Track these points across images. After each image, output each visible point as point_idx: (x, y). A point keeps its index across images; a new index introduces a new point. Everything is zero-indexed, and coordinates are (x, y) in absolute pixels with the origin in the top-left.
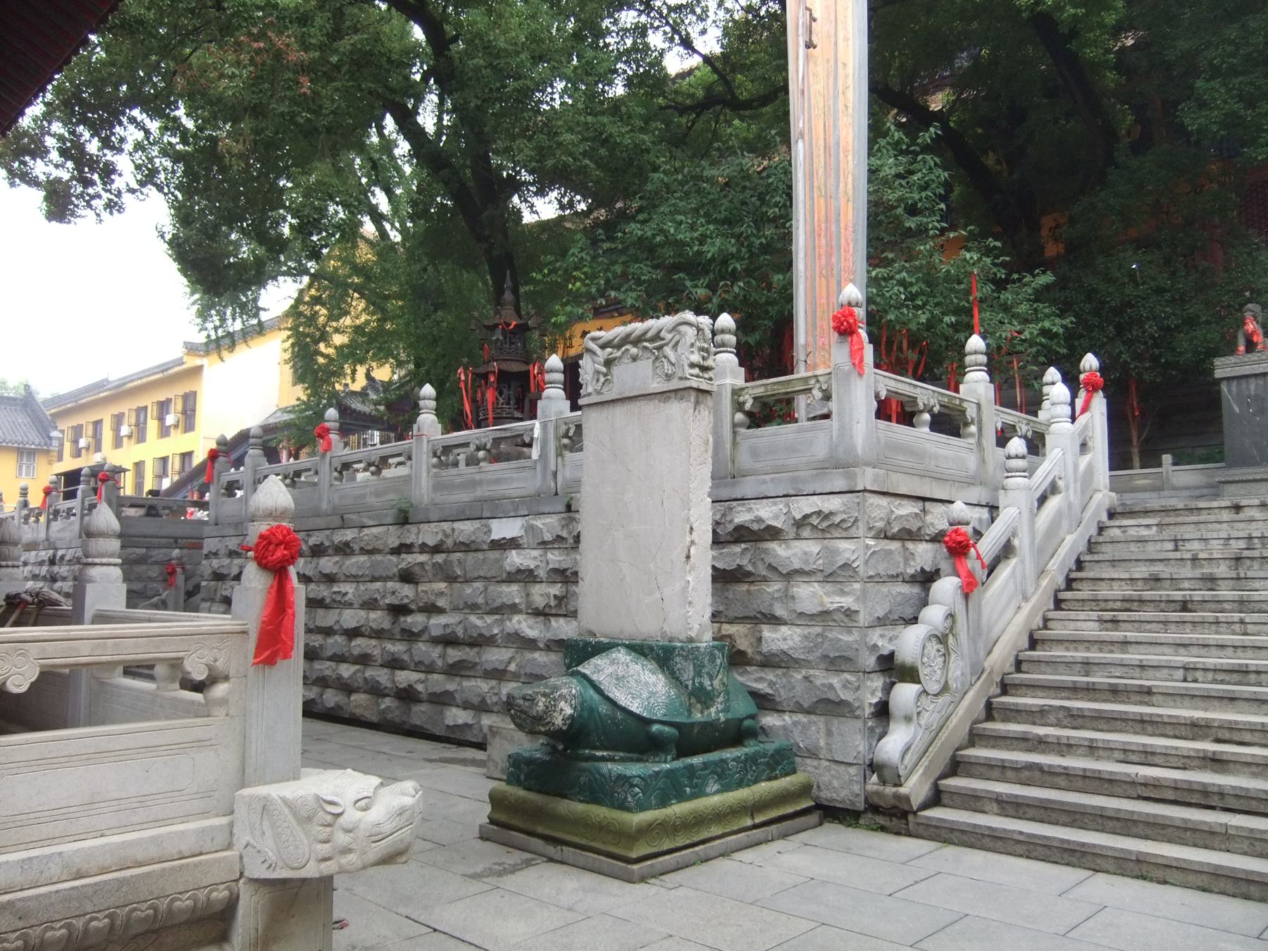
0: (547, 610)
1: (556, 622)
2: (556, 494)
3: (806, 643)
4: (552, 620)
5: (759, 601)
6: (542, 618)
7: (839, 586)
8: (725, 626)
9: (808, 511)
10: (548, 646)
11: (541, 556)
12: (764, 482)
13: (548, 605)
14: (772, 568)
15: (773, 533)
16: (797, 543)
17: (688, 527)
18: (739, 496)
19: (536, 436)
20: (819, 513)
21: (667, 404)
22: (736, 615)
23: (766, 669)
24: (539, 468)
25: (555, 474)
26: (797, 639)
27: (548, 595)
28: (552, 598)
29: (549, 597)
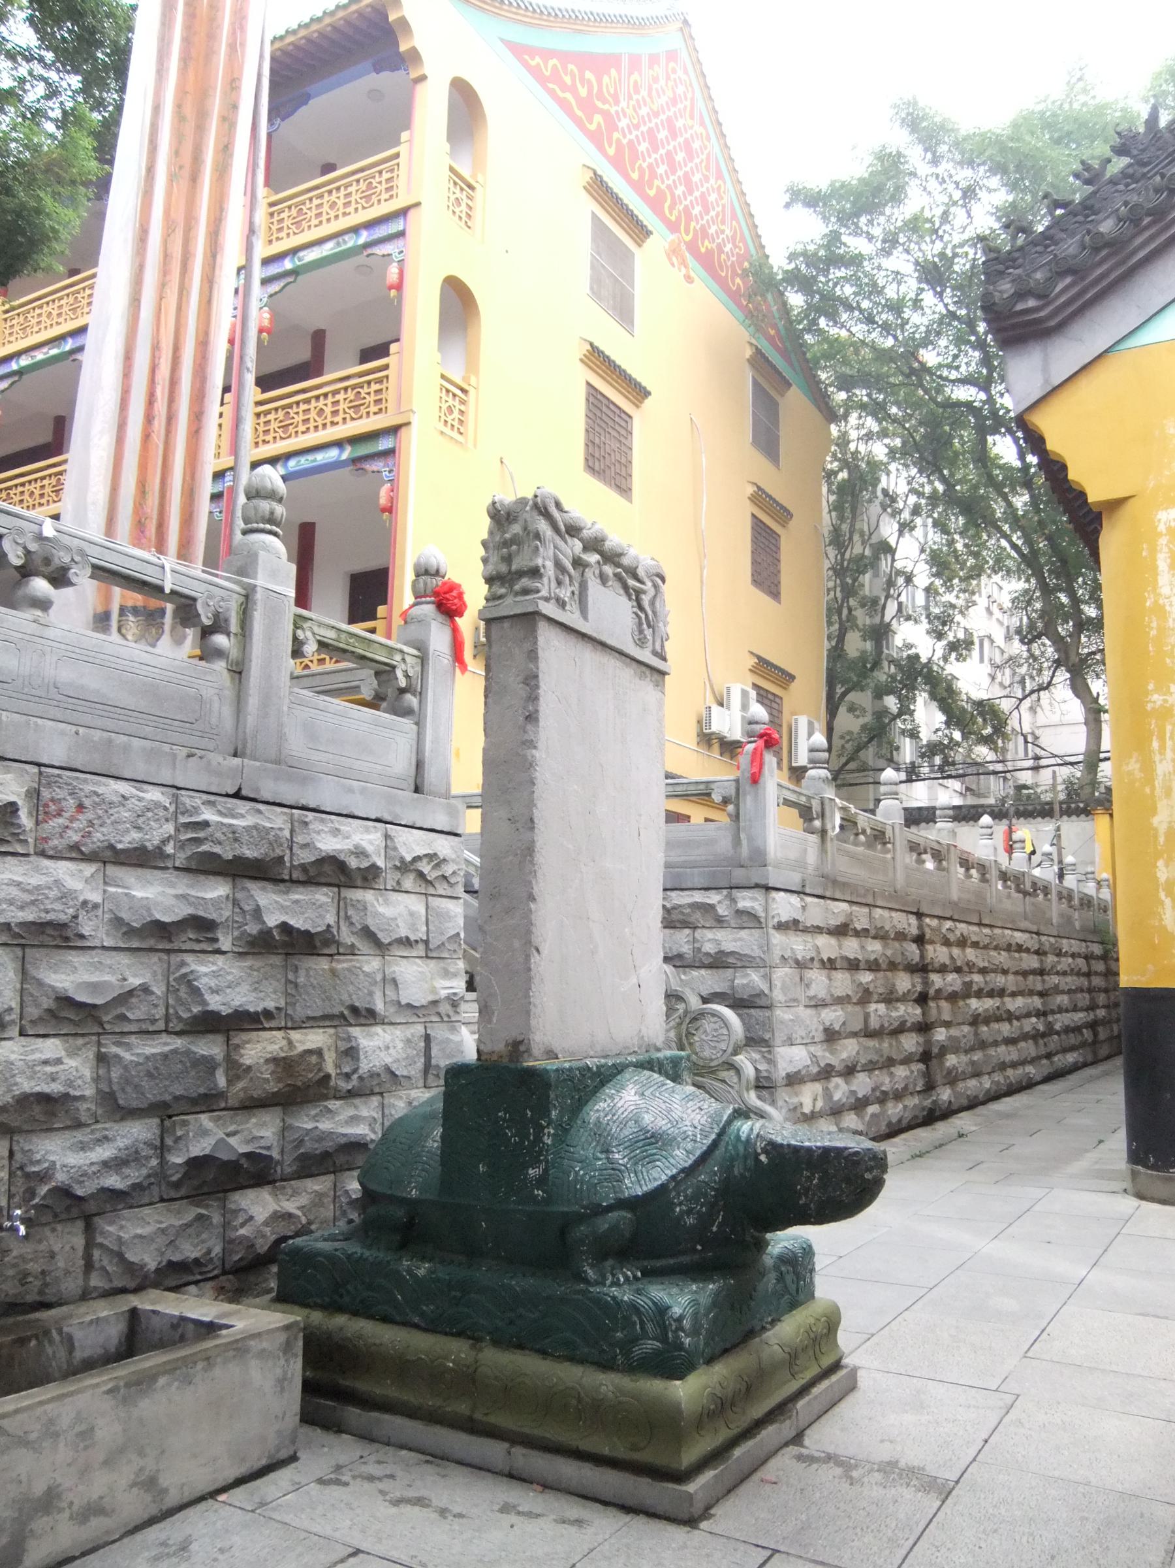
3: (409, 1051)
5: (351, 988)
7: (442, 964)
8: (295, 1035)
9: (421, 851)
12: (351, 790)
14: (368, 934)
15: (369, 876)
16: (395, 896)
18: (312, 805)
20: (431, 857)
22: (310, 1013)
23: (357, 1101)
26: (400, 1045)
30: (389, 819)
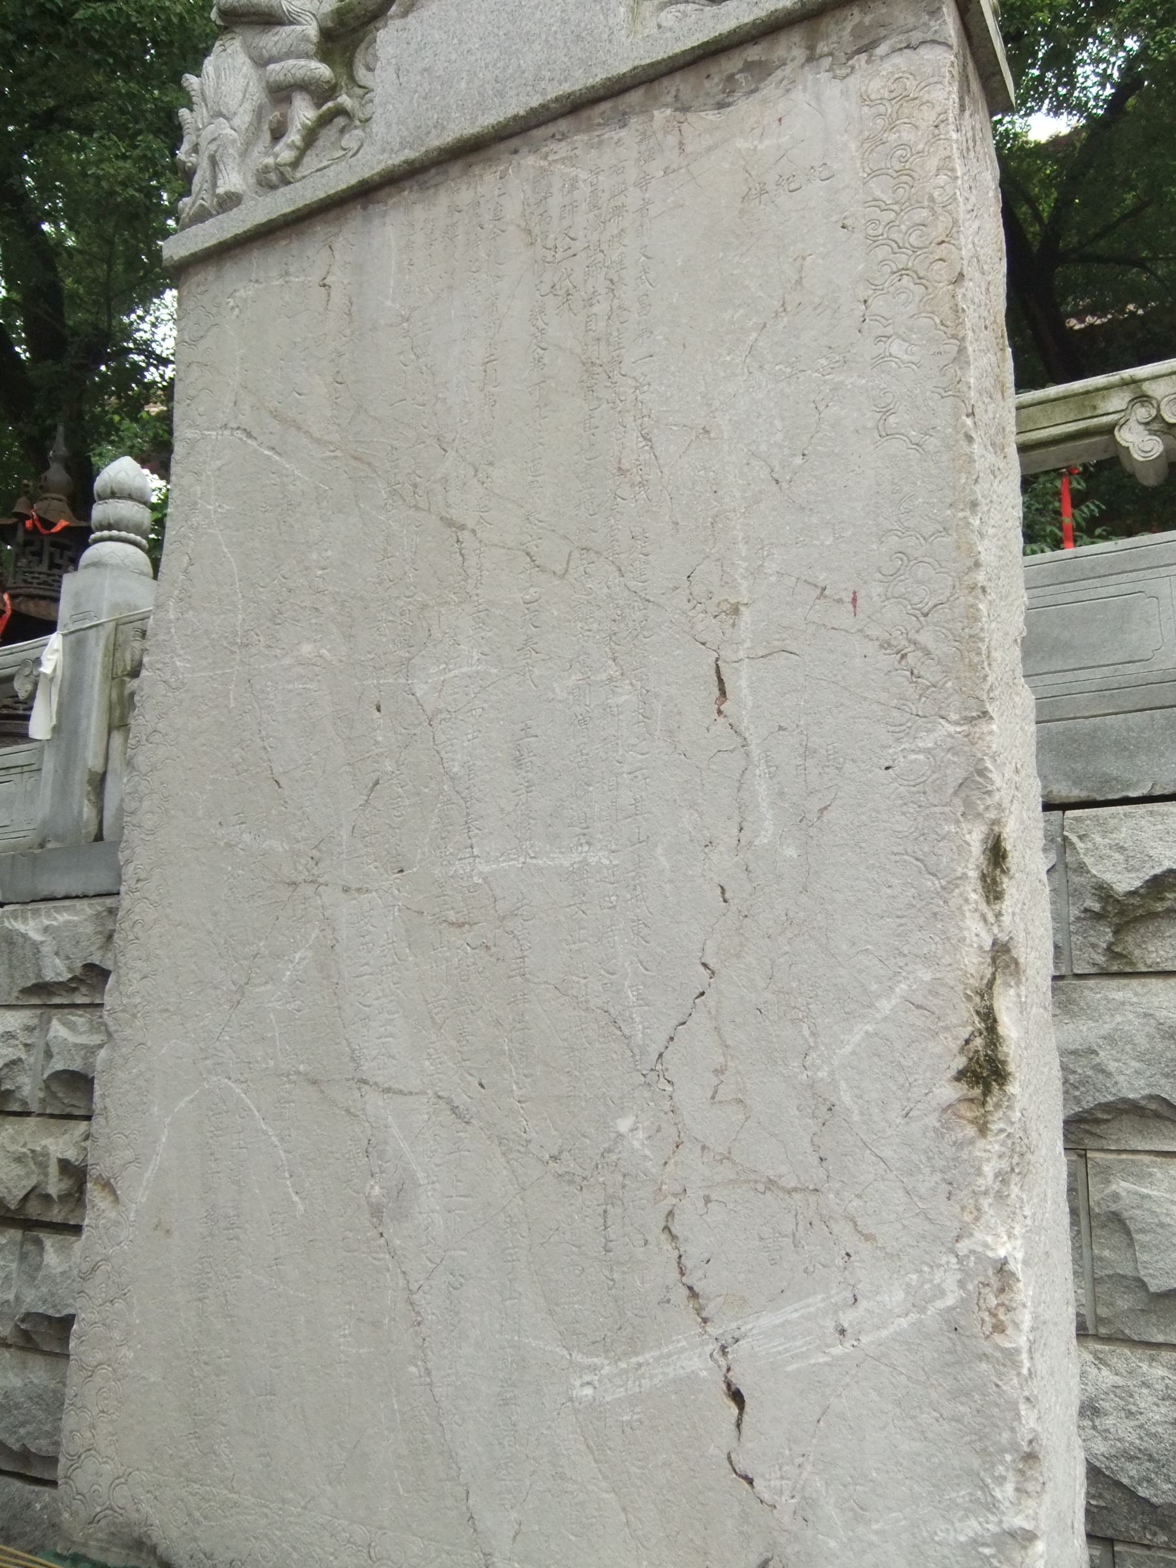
0: (34, 1210)
1: (63, 1250)
2: (99, 837)
4: (50, 1242)
6: (15, 1234)
10: (26, 1334)
11: (29, 1029)
13: (35, 1193)
17: (975, 838)
19: (47, 668)
21: (744, 108)
24: (49, 765)
25: (98, 783)
27: (39, 1159)
28: (53, 1169)
29: (43, 1166)
30: (1077, 794)
